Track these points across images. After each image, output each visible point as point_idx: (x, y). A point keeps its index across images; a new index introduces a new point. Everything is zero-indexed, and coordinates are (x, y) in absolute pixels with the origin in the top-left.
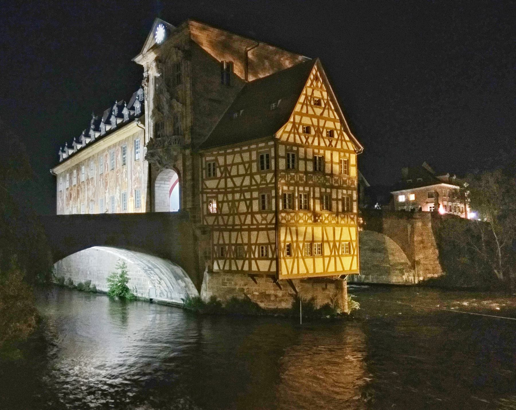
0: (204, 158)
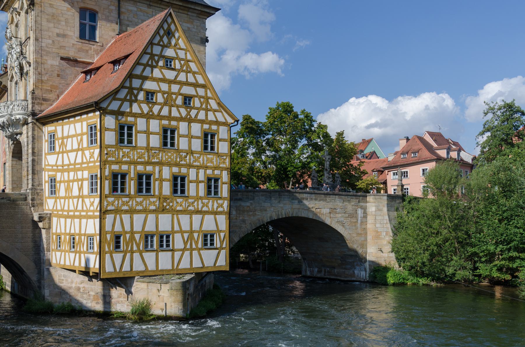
0: (46, 128)
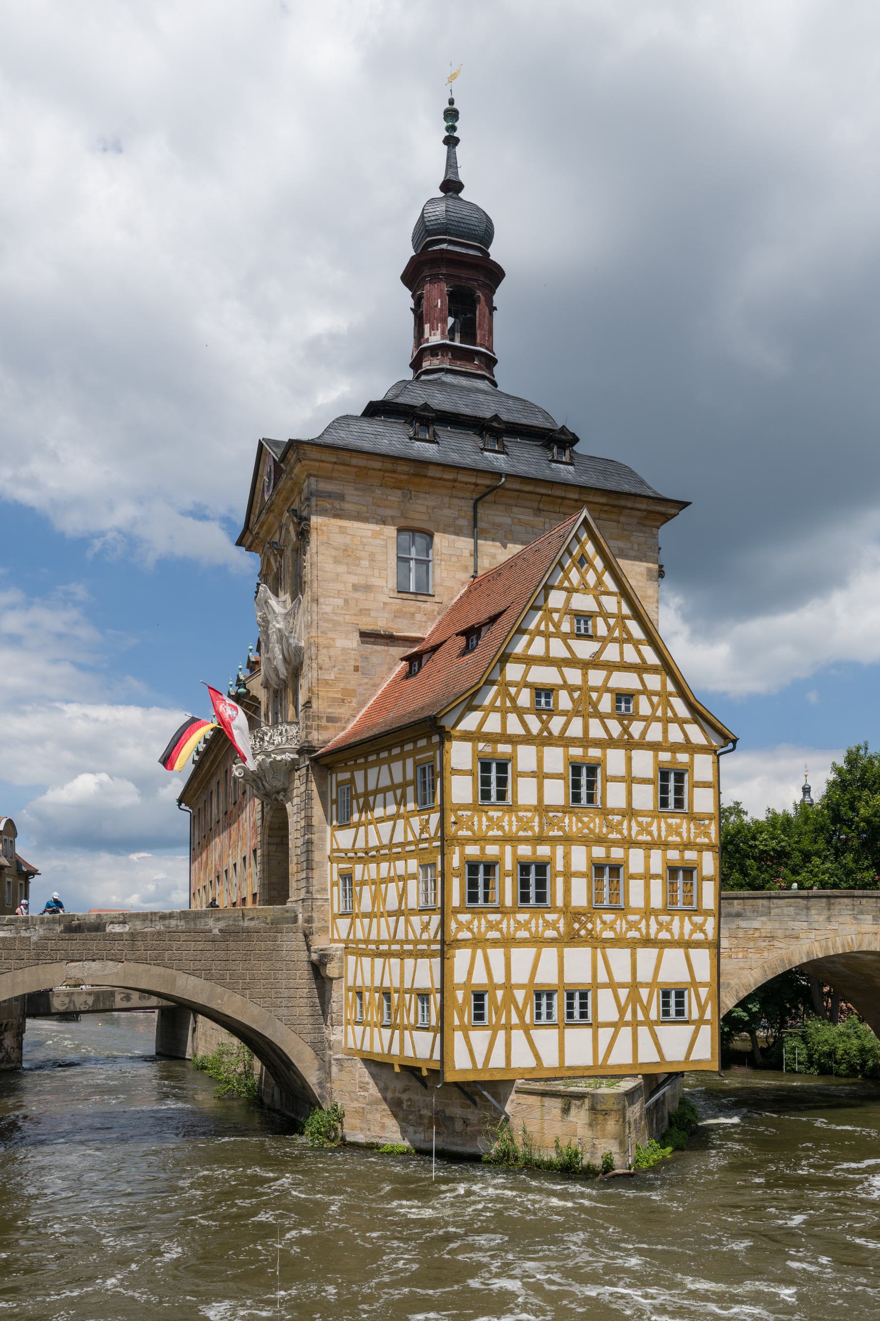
0: (334, 776)
